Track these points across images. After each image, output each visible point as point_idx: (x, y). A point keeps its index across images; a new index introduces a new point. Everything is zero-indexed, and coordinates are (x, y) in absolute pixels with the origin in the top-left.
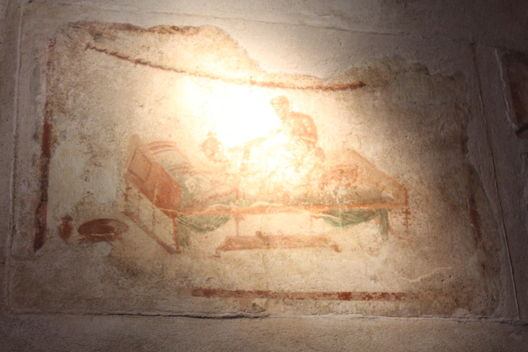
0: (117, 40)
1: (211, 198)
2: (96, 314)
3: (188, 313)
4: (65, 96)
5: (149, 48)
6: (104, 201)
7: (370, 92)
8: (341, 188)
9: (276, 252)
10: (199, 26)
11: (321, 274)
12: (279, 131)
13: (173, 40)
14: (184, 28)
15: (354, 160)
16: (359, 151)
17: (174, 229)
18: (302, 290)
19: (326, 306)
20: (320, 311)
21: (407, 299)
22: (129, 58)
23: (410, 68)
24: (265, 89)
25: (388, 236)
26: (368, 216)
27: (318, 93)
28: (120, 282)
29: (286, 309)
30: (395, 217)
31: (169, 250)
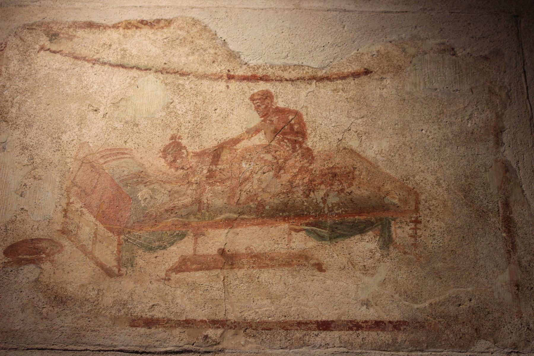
0: (76, 40)
1: (167, 211)
2: (10, 349)
3: (122, 348)
4: (10, 104)
5: (110, 45)
6: (39, 219)
7: (377, 80)
8: (331, 194)
9: (240, 273)
10: (171, 18)
11: (296, 300)
12: (257, 130)
15: (352, 161)
16: (358, 150)
19: (300, 338)
20: (292, 344)
21: (408, 328)
22: (87, 58)
23: (432, 49)
24: (245, 84)
25: (389, 251)
28: (44, 310)
29: (247, 343)
30: (400, 227)
31: (109, 273)
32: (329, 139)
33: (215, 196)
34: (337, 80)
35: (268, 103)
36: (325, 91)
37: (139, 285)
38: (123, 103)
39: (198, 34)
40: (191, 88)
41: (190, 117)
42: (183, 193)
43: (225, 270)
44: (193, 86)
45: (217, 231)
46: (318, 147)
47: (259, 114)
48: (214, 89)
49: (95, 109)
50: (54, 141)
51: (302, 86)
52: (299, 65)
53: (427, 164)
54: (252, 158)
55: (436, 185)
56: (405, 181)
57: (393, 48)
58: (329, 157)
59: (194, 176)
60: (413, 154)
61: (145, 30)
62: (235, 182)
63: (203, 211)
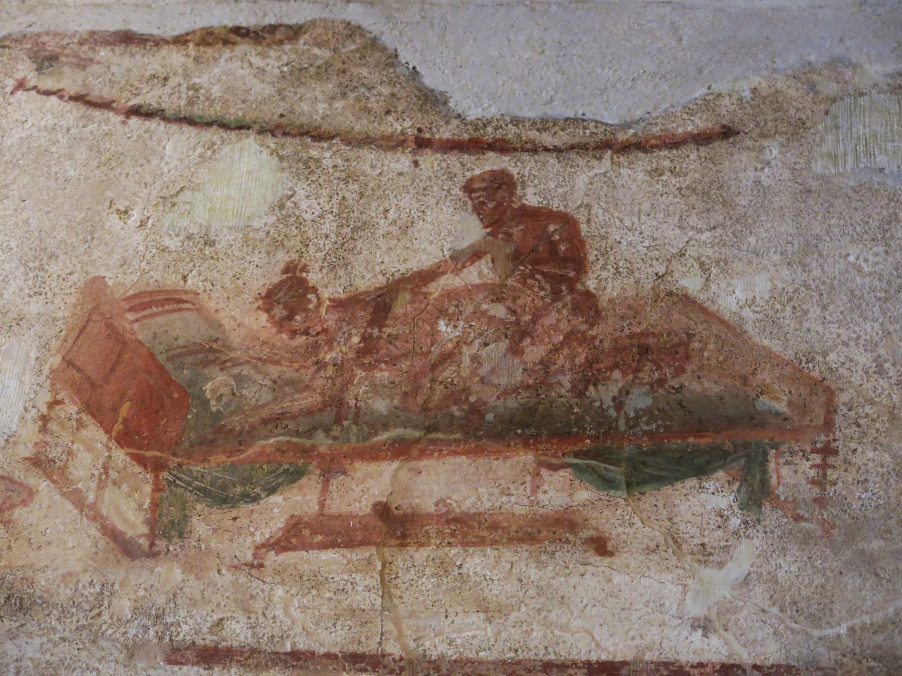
0: (94, 68)
1: (265, 422)
5: (166, 79)
8: (636, 391)
9: (421, 555)
10: (301, 22)
11: (543, 614)
12: (475, 255)
13: (231, 59)
14: (264, 29)
15: (685, 320)
16: (702, 297)
17: (153, 499)
18: (482, 654)
22: (114, 105)
24: (453, 160)
26: (709, 462)
27: (600, 159)
30: (787, 463)
31: (127, 549)
32: (637, 275)
33: (374, 392)
34: (660, 150)
35: (504, 198)
36: (629, 171)
37: (193, 577)
38: (187, 196)
39: (358, 55)
40: (335, 166)
41: (329, 225)
42: (302, 386)
43: (386, 549)
44: (339, 162)
45: (373, 467)
46: (608, 291)
47: (481, 220)
48: (386, 168)
49: (123, 209)
50: (31, 275)
51: (582, 162)
52: (575, 120)
53: (857, 329)
54: (461, 313)
55: (875, 372)
56: (803, 364)
57: (788, 83)
58: (634, 310)
59: (331, 349)
60: (824, 308)
61: (243, 47)
62: (418, 363)
63: (345, 423)
